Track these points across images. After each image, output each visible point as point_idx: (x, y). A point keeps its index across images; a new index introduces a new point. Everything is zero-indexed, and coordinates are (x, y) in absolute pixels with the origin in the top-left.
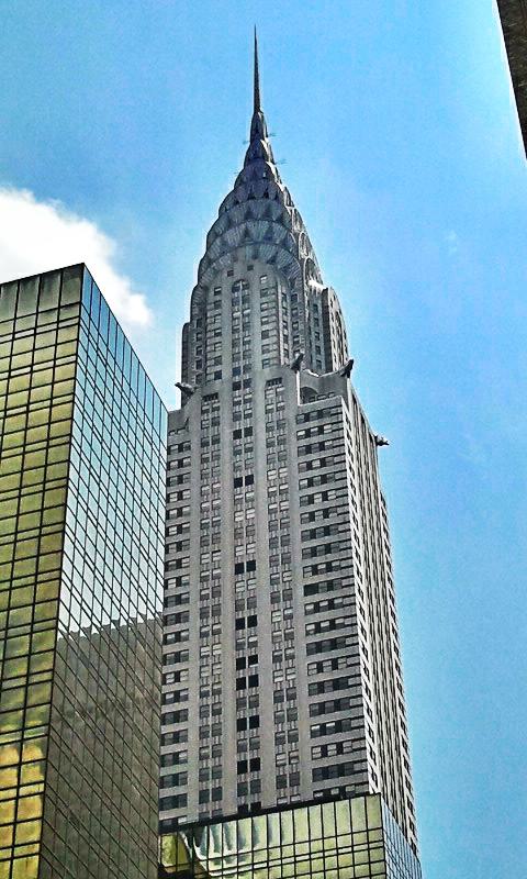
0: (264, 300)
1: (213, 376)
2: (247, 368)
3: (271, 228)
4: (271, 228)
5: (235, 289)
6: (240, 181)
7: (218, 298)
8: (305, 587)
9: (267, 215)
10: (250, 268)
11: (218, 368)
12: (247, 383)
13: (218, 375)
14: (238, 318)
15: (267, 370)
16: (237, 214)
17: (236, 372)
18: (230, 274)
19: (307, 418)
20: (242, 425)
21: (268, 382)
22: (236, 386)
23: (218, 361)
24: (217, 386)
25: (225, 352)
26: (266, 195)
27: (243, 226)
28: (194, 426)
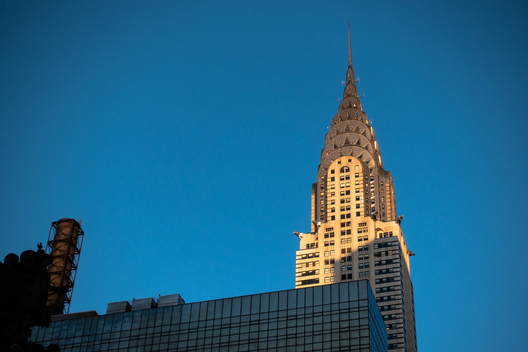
1: (330, 218)
2: (349, 216)
7: (333, 175)
10: (350, 161)
11: (333, 214)
12: (349, 224)
13: (333, 218)
14: (344, 187)
15: (358, 217)
17: (343, 217)
18: (339, 163)
22: (343, 225)
23: (333, 211)
24: (331, 224)
25: (338, 206)
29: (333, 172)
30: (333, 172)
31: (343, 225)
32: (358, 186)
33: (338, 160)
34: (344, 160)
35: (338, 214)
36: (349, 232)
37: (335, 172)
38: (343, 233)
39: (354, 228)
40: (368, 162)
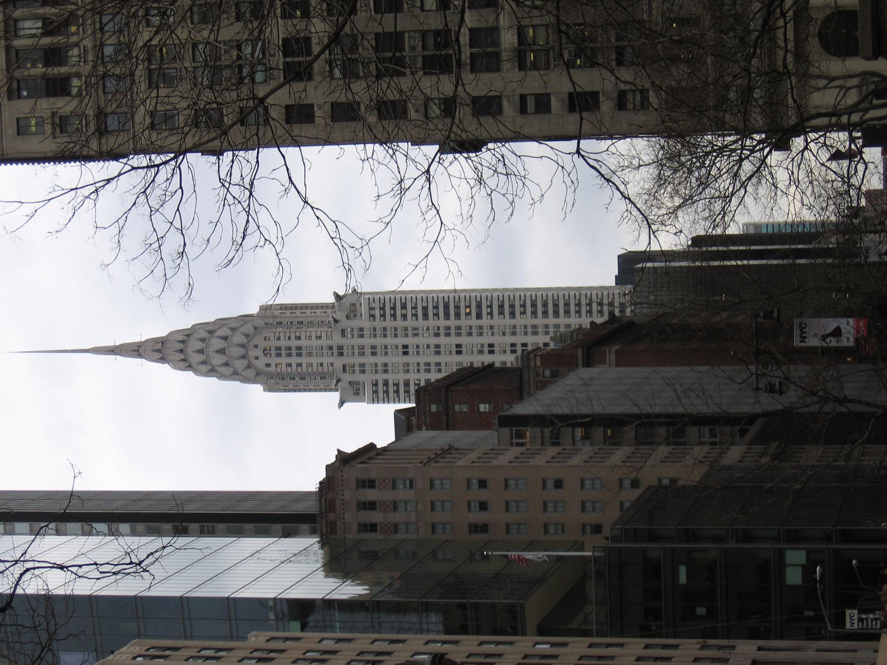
0: (282, 338)
2: (331, 348)
3: (219, 337)
4: (219, 337)
6: (163, 360)
7: (273, 365)
8: (477, 318)
9: (203, 340)
10: (256, 346)
16: (195, 358)
18: (257, 358)
19: (373, 316)
20: (368, 351)
22: (341, 354)
26: (183, 342)
27: (211, 354)
28: (358, 377)
29: (268, 365)
30: (268, 365)
31: (341, 354)
32: (293, 338)
33: (253, 360)
34: (253, 353)
35: (326, 360)
37: (268, 362)
40: (256, 328)
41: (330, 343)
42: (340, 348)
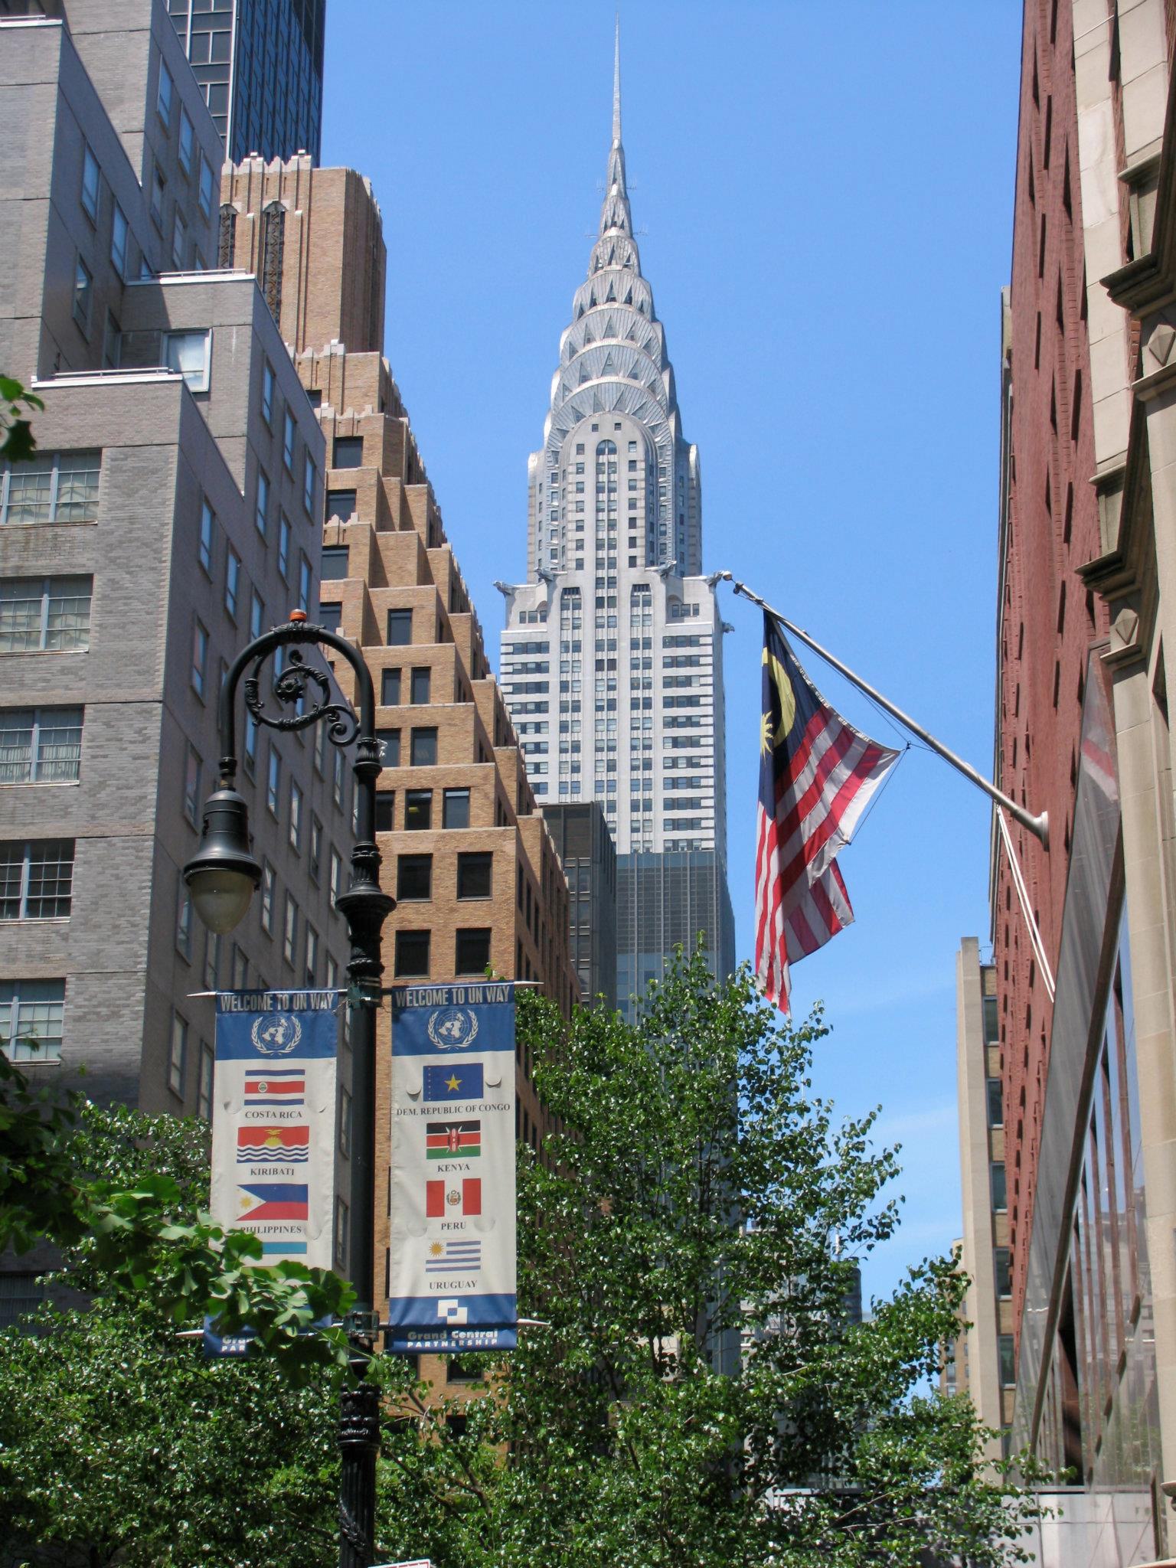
1: (573, 565)
5: (600, 452)
11: (580, 554)
13: (580, 564)
18: (595, 428)
21: (635, 586)
29: (580, 448)
30: (580, 448)
31: (599, 582)
36: (612, 601)
38: (599, 603)
39: (624, 592)
41: (623, 562)
42: (612, 582)
